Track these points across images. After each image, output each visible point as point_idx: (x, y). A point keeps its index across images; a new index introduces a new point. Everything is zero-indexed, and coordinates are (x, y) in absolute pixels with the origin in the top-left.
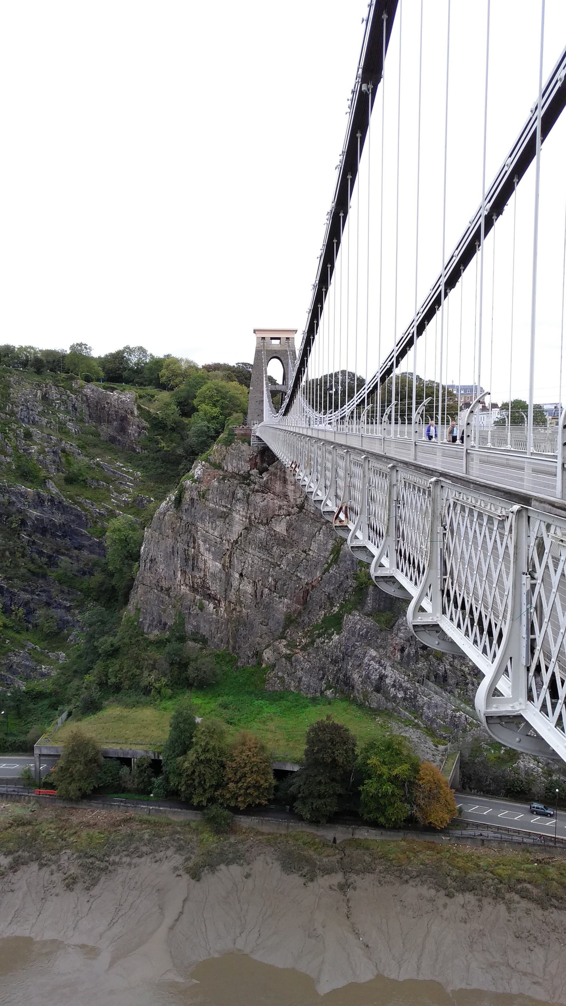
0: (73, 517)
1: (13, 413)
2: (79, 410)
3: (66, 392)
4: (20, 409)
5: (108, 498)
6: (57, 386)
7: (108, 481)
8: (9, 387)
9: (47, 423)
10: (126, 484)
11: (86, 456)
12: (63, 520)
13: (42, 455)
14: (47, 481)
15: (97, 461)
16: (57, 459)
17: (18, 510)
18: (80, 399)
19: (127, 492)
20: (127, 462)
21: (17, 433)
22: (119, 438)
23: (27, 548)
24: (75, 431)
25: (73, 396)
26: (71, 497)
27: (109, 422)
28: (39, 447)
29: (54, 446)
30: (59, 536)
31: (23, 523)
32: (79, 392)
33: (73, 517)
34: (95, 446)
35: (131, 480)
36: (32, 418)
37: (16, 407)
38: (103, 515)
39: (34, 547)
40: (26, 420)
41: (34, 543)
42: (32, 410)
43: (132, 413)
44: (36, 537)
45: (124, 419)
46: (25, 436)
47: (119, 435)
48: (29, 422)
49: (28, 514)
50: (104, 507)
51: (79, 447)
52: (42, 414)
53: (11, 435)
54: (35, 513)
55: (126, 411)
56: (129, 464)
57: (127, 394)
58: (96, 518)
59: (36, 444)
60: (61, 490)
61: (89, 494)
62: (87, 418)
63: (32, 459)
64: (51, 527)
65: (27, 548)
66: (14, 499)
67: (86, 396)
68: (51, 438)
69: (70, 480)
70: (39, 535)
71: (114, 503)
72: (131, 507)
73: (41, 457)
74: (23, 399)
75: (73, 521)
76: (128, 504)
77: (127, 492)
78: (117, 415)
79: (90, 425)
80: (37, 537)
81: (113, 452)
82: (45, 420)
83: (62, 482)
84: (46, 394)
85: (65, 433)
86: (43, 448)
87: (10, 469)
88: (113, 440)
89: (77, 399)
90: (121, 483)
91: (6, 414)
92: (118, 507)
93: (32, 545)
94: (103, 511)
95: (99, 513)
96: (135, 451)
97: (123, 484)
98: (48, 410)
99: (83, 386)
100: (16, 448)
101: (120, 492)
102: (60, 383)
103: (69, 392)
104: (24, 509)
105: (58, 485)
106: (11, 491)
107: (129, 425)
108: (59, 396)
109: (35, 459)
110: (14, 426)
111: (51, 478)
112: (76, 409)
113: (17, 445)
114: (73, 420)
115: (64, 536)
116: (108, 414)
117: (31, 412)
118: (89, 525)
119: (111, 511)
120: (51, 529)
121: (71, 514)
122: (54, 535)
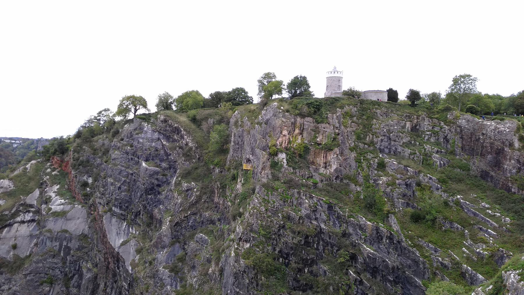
0: (409, 262)
1: (372, 143)
2: (451, 141)
3: (440, 123)
4: (379, 139)
5: (458, 246)
6: (431, 118)
7: (465, 223)
8: (373, 118)
9: (411, 154)
10: (486, 231)
11: (445, 191)
12: (398, 263)
13: (390, 187)
14: (390, 215)
15: (458, 199)
16: (410, 193)
17: (352, 244)
18: (454, 131)
19: (485, 242)
20: (496, 203)
21: (370, 164)
22: (493, 173)
23: (354, 287)
24: (440, 164)
25: (447, 127)
26: (411, 238)
27: (482, 155)
28: (390, 178)
29: (409, 178)
30: (390, 281)
31: (353, 258)
32: (453, 123)
33: (409, 262)
34: (460, 181)
35: (495, 227)
36: (394, 148)
37: (376, 137)
38: (446, 266)
39: (360, 287)
40: (387, 151)
41: (361, 282)
42: (395, 141)
43: (511, 145)
44: (366, 276)
45: (500, 152)
46: (378, 167)
47: (493, 170)
48: (390, 152)
49: (362, 249)
50: (450, 256)
51: (439, 181)
52: (407, 145)
53: (364, 164)
54: (368, 249)
55: (503, 143)
56: (498, 206)
57: (506, 123)
58: (437, 269)
59: (387, 175)
60: (403, 228)
61: (434, 237)
62: (458, 151)
63: (378, 190)
64: (384, 269)
65: (354, 287)
66: (351, 230)
67: (460, 127)
68: (407, 170)
69: (417, 218)
70: (368, 275)
71: (464, 252)
72: (487, 264)
73: (388, 190)
74: (385, 130)
75: (410, 267)
76: (483, 258)
77: (485, 242)
78: (492, 148)
79: (461, 158)
80: (366, 277)
81: (481, 189)
82: (408, 151)
83: (407, 218)
84: (416, 126)
85: (429, 165)
86: (394, 178)
87: (358, 198)
88: (484, 175)
89: (450, 131)
90: (481, 229)
91: (365, 144)
92: (468, 259)
93: (359, 285)
94: (447, 262)
95: (441, 263)
96: (509, 190)
97: (483, 230)
98: (415, 141)
99: (457, 117)
100: (367, 178)
101: (476, 240)
102: (434, 115)
103: (442, 124)
104: (359, 244)
105: (401, 223)
106: (350, 222)
107: (506, 159)
108: (430, 128)
109: (382, 190)
110: (370, 156)
111: (394, 213)
112: (448, 141)
113: (369, 175)
114: (441, 152)
115: (395, 282)
116: (483, 147)
117: (393, 143)
118: (426, 276)
119: (457, 263)
120: (383, 271)
121: (408, 258)
122: (384, 279)
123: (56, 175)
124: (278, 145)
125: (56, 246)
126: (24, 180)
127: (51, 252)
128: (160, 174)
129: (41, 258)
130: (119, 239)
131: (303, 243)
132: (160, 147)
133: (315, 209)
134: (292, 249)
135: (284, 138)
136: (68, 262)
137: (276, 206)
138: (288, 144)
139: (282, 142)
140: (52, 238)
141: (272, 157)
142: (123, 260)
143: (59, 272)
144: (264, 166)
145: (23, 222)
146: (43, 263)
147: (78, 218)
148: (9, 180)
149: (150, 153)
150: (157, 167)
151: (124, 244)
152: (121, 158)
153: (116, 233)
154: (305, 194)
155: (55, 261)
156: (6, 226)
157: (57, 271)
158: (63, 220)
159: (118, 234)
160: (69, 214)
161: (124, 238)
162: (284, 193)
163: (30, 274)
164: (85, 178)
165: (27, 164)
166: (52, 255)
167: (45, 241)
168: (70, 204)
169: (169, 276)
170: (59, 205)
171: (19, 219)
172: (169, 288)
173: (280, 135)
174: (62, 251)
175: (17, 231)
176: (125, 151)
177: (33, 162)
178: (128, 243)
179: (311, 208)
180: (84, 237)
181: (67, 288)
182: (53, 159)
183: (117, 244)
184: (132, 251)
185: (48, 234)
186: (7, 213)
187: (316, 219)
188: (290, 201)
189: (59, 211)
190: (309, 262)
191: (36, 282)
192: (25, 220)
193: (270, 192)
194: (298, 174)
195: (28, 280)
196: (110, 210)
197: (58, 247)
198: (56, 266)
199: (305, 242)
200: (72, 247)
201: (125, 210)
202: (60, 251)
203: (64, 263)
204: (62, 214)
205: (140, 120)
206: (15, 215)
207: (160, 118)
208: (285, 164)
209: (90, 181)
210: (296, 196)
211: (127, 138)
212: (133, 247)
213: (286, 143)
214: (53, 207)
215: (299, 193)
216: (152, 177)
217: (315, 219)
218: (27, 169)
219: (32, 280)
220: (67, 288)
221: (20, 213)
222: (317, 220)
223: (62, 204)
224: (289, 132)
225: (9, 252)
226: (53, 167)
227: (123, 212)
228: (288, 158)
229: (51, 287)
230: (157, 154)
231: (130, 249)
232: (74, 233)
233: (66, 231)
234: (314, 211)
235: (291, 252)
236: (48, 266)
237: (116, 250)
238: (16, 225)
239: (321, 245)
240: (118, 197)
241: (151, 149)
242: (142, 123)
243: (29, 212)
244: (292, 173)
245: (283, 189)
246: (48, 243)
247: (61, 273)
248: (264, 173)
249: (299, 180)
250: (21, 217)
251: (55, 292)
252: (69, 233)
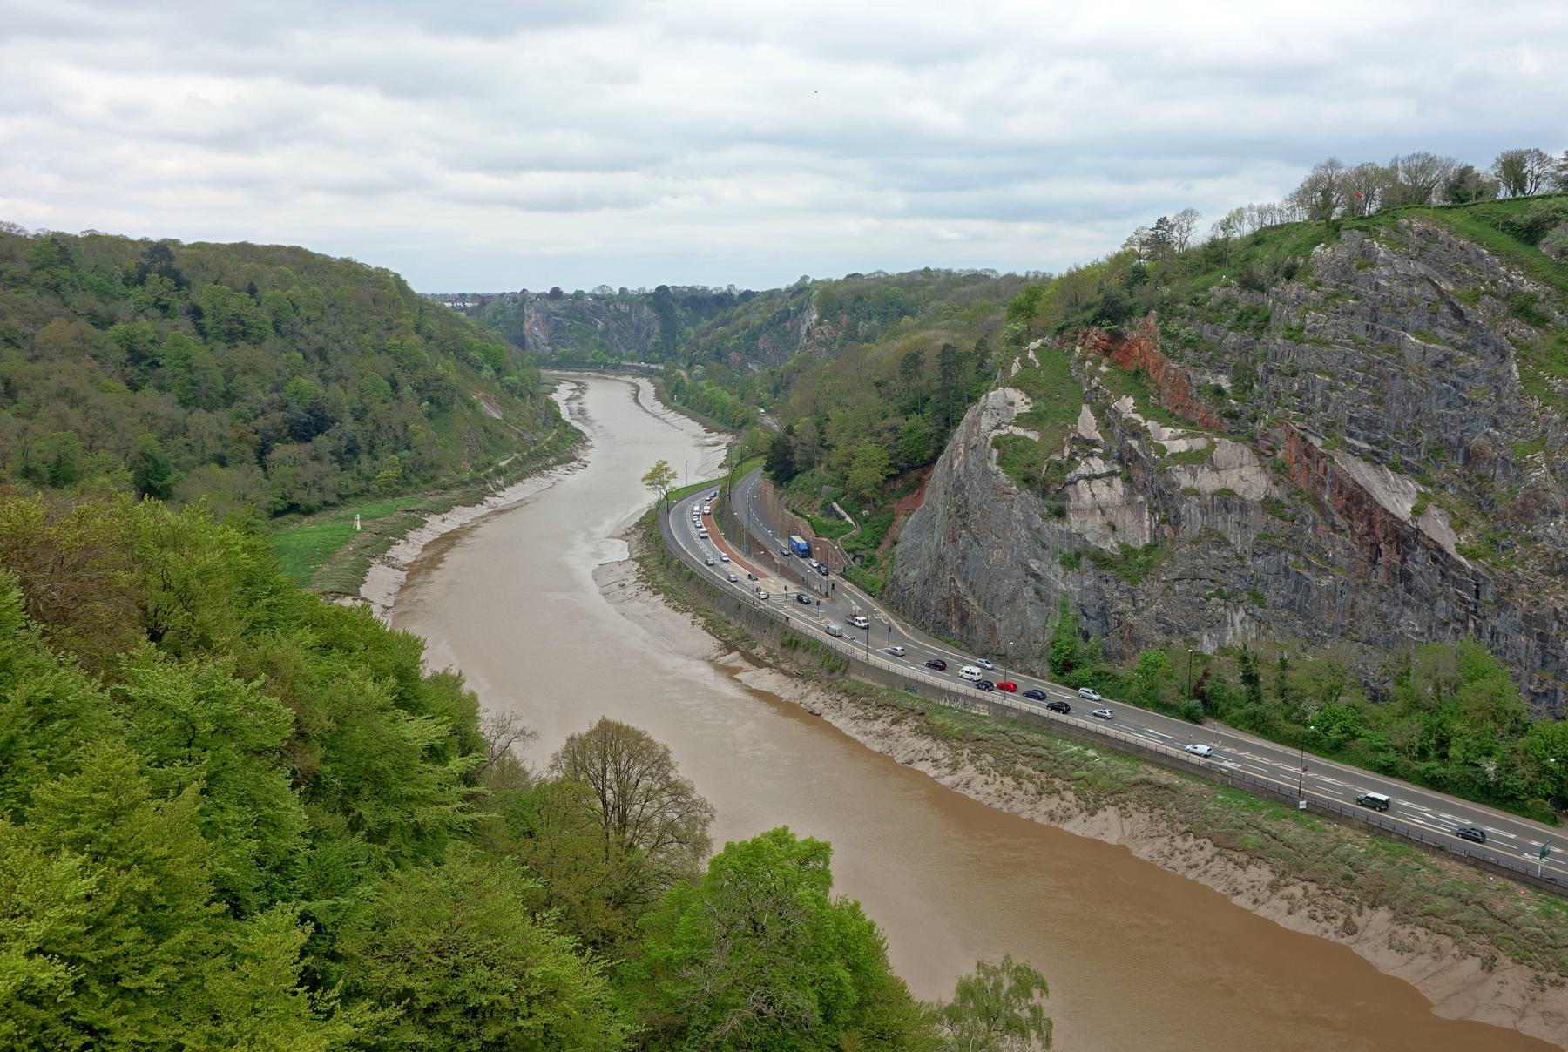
132: (1435, 297)
142: (1432, 545)
145: (1090, 478)
147: (1241, 466)
151: (1417, 512)
152: (1335, 326)
163: (1179, 579)
164: (1208, 376)
171: (1083, 469)
175: (1093, 495)
176: (1340, 310)
180: (1270, 505)
182: (1085, 336)
185: (1195, 500)
186: (1057, 457)
191: (1197, 596)
195: (1181, 593)
204: (1193, 459)
207: (1410, 227)
209: (1224, 382)
214: (1165, 443)
219: (1188, 593)
223: (1180, 437)
225: (1105, 538)
237: (1410, 523)
240: (1355, 415)
243: (1091, 455)
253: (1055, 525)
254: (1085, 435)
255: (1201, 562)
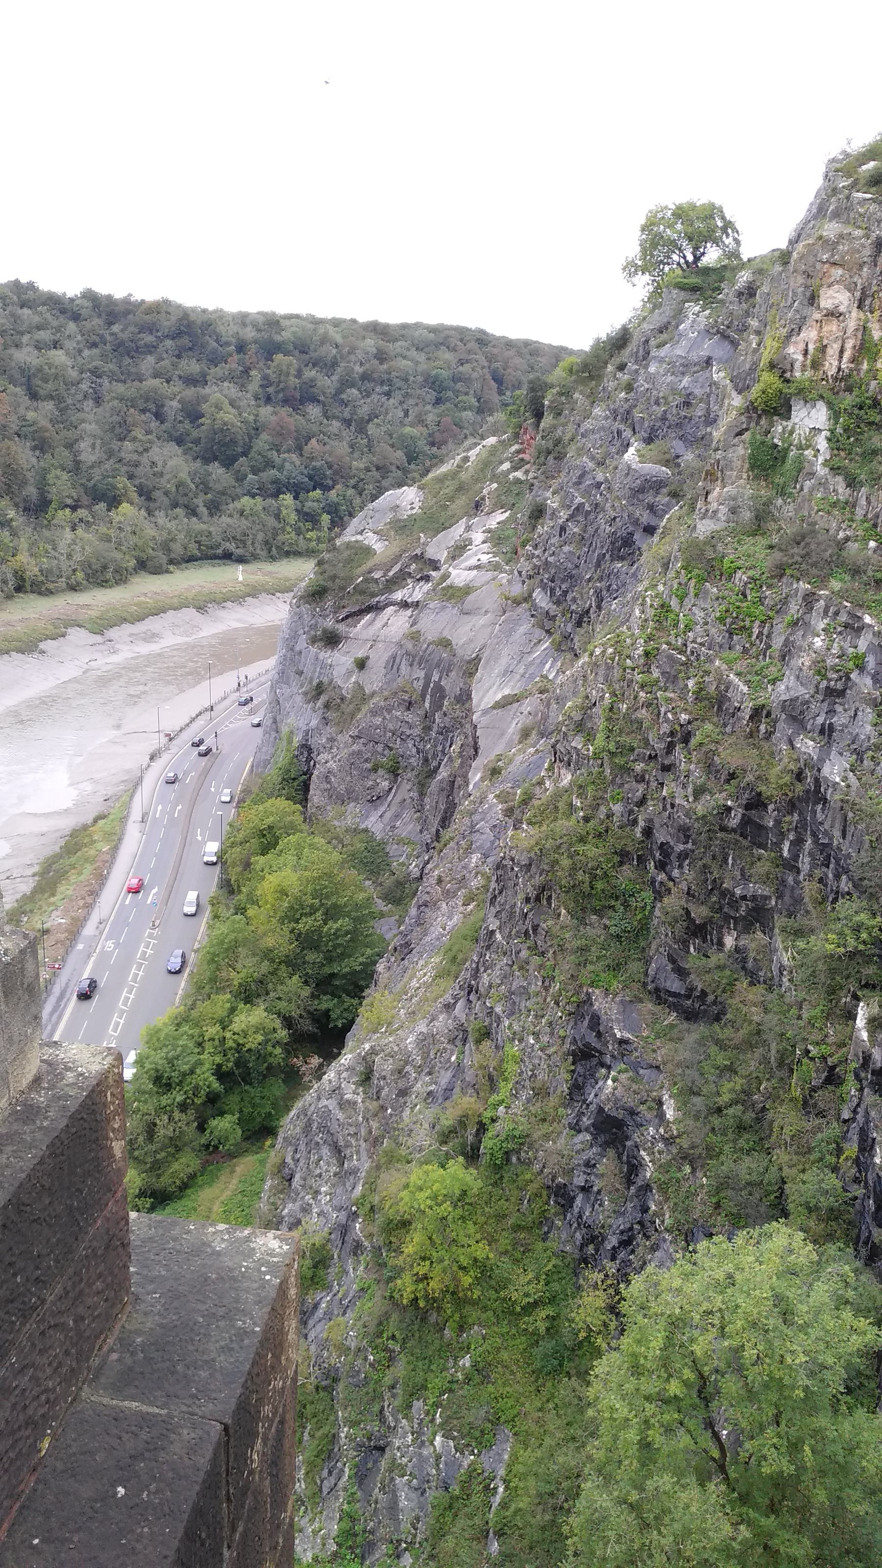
123: (518, 481)
124: (797, 366)
125: (418, 679)
126: (447, 491)
127: (406, 692)
128: (664, 491)
129: (382, 703)
130: (501, 689)
131: (734, 821)
133: (839, 686)
134: (687, 837)
135: (832, 327)
136: (435, 728)
137: (690, 646)
138: (853, 360)
139: (823, 349)
140: (414, 657)
141: (763, 422)
143: (414, 750)
144: (718, 461)
145: (405, 605)
146: (384, 718)
147: (486, 612)
148: (419, 488)
149: (665, 412)
150: (667, 463)
153: (503, 668)
154: (832, 610)
155: (409, 717)
156: (369, 609)
157: (410, 746)
158: (455, 611)
159: (508, 672)
160: (471, 598)
161: (513, 687)
162: (748, 592)
165: (476, 444)
166: (404, 700)
167: (398, 660)
168: (496, 567)
169: (495, 826)
170: (470, 569)
171: (398, 596)
172: (474, 860)
173: (808, 311)
174: (428, 697)
177: (492, 440)
178: (516, 705)
179: (824, 677)
181: (422, 794)
183: (486, 700)
184: (511, 731)
186: (377, 575)
187: (827, 732)
188: (761, 634)
189: (461, 585)
190: (742, 911)
191: (366, 761)
192: (409, 600)
193: (692, 583)
194: (859, 512)
195: (353, 753)
196: (528, 598)
197: (421, 683)
198: (408, 732)
199: (746, 821)
200: (447, 688)
201: (558, 603)
202: (423, 696)
203: (427, 729)
205: (683, 293)
206: (395, 583)
208: (821, 459)
210: (794, 609)
211: (636, 362)
212: (522, 716)
213: (847, 355)
215: (809, 600)
216: (639, 500)
217: (822, 732)
218: (466, 459)
219: (359, 753)
220: (422, 794)
221: (409, 581)
222: (830, 736)
223: (478, 567)
224: (858, 294)
226: (521, 456)
227: (553, 609)
228: (839, 430)
229: (395, 781)
230: (685, 417)
231: (511, 722)
232: (460, 652)
233: (445, 643)
234: (830, 692)
235: (681, 847)
236: (391, 726)
238: (390, 610)
239: (806, 853)
240: (551, 559)
241: (671, 398)
242: (687, 305)
244: (834, 505)
245: (751, 573)
246: (404, 669)
247: (418, 753)
248: (720, 495)
249: (847, 539)
250: (405, 591)
251: (399, 798)
252: (452, 649)
253: (313, 650)
254: (432, 552)
255: (378, 720)
